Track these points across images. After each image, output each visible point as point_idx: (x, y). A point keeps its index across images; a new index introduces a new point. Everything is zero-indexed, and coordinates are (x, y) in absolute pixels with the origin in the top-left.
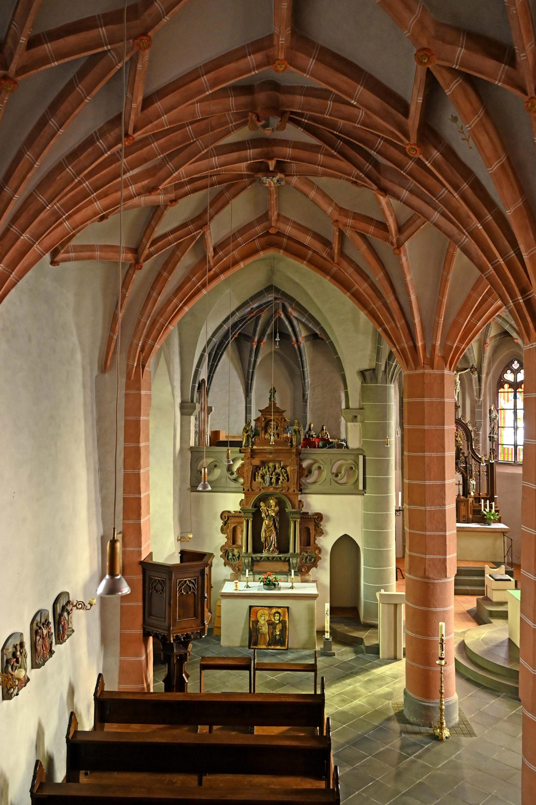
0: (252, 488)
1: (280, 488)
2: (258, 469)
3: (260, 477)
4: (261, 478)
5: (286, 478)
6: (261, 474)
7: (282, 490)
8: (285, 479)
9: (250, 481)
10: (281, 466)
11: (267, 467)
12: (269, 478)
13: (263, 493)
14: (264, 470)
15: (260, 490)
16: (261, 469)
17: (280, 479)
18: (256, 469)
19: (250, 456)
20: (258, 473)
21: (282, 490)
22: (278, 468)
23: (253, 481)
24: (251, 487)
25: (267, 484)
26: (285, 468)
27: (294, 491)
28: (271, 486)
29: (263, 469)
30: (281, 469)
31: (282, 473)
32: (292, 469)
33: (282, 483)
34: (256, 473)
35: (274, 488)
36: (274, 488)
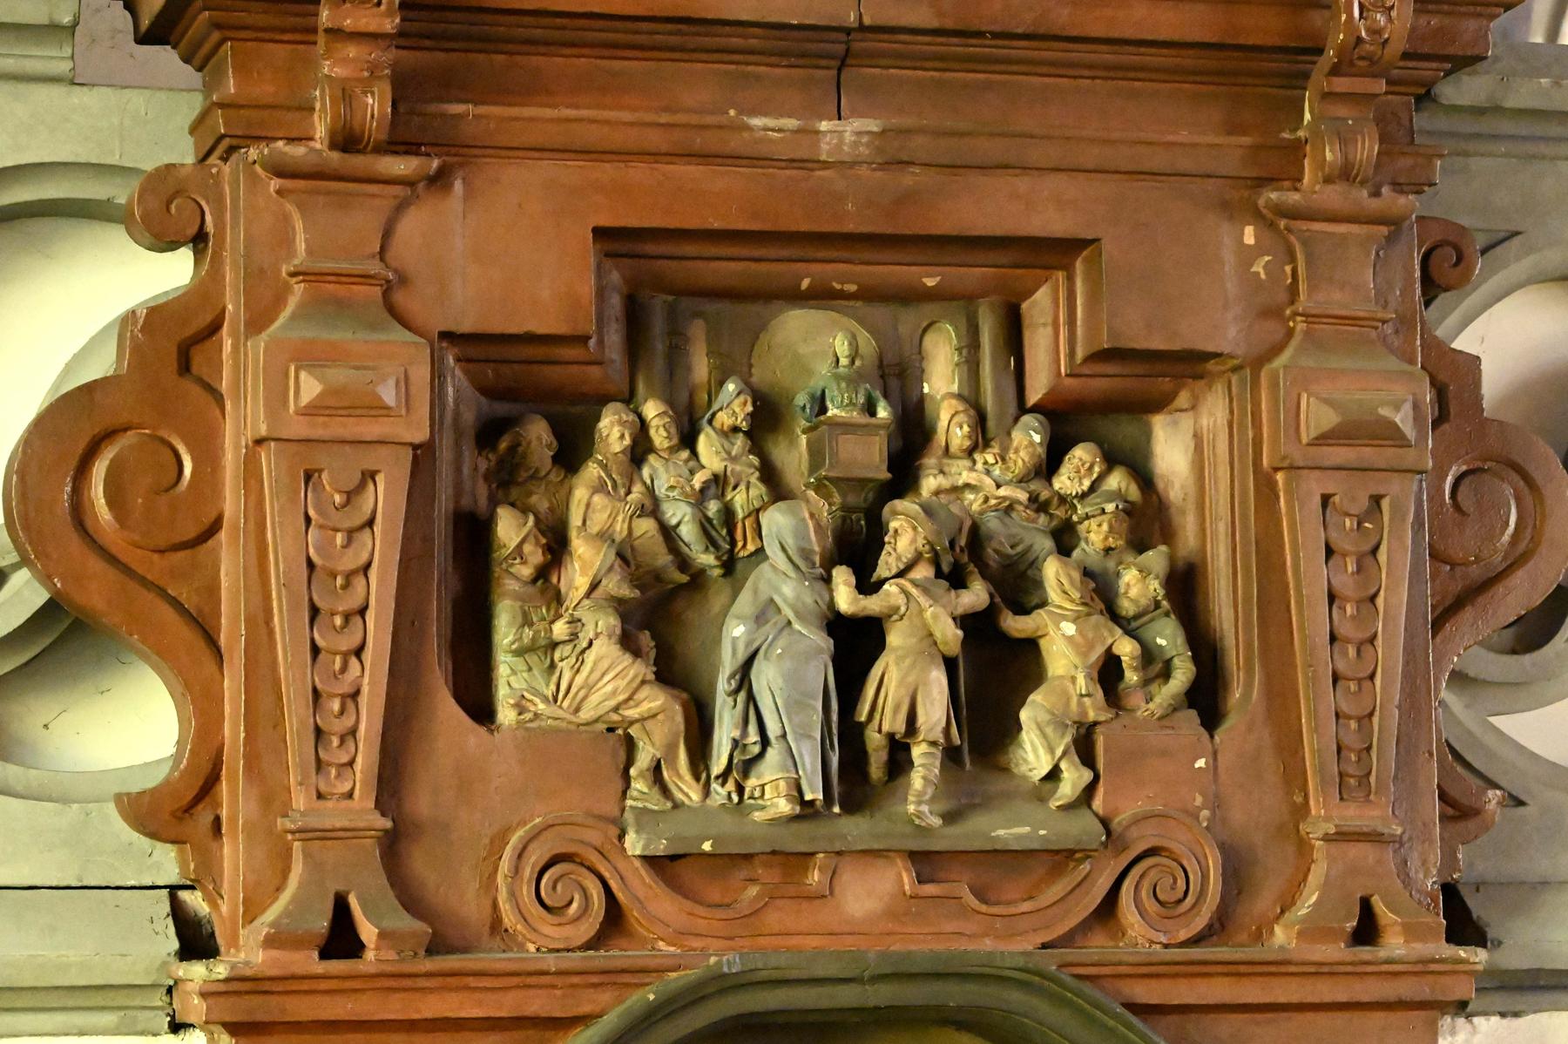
0: (421, 863)
1: (1060, 858)
2: (538, 435)
3: (601, 624)
4: (627, 642)
5: (1167, 636)
6: (625, 555)
7: (1109, 906)
8: (1155, 665)
9: (369, 718)
10: (1034, 396)
11: (733, 407)
12: (823, 643)
13: (693, 996)
14: (661, 473)
15: (615, 919)
16: (612, 430)
17: (1027, 655)
18: (488, 433)
19: (375, 105)
20: (556, 545)
21: (1109, 906)
22: (982, 436)
23: (447, 710)
24: (392, 847)
25: (770, 775)
26: (1123, 430)
27: (1367, 931)
28: (855, 829)
29: (640, 450)
30: (1029, 438)
31: (1065, 539)
32: (1317, 416)
33: (1084, 748)
34: (509, 529)
35: (926, 862)
36: (926, 862)
